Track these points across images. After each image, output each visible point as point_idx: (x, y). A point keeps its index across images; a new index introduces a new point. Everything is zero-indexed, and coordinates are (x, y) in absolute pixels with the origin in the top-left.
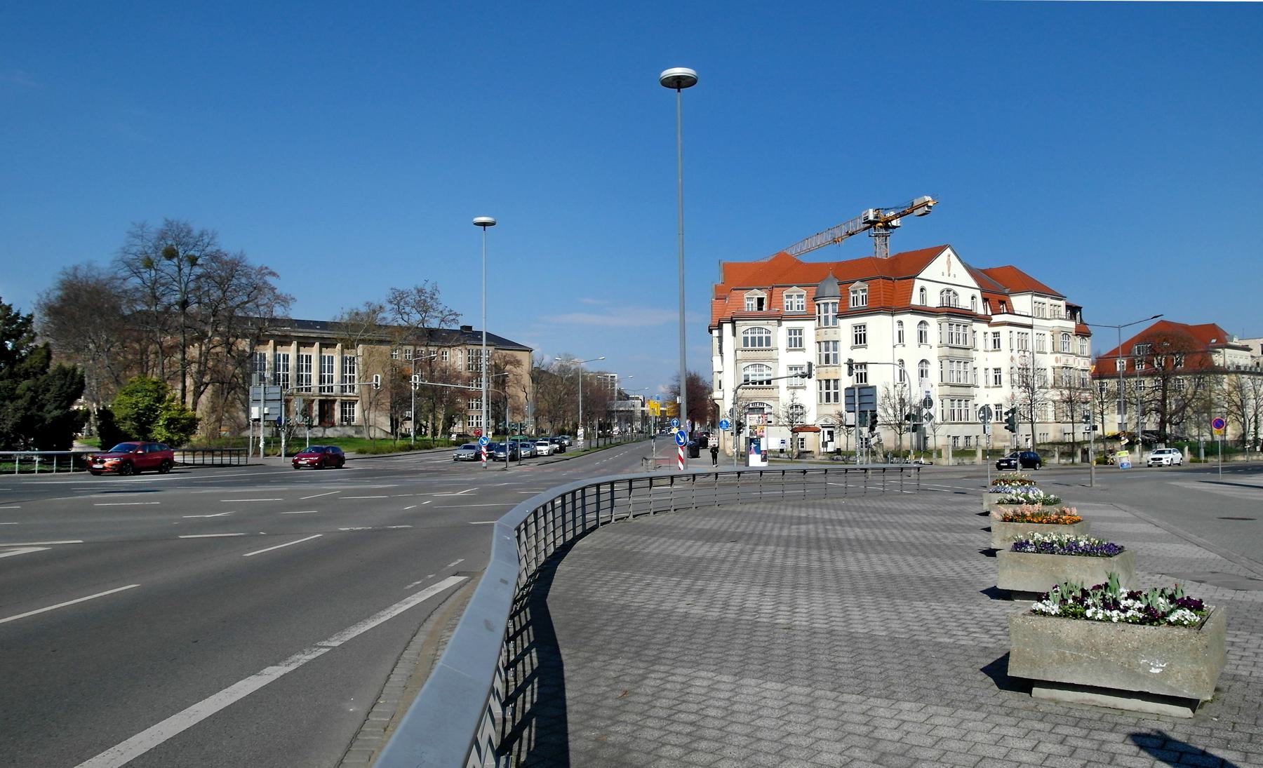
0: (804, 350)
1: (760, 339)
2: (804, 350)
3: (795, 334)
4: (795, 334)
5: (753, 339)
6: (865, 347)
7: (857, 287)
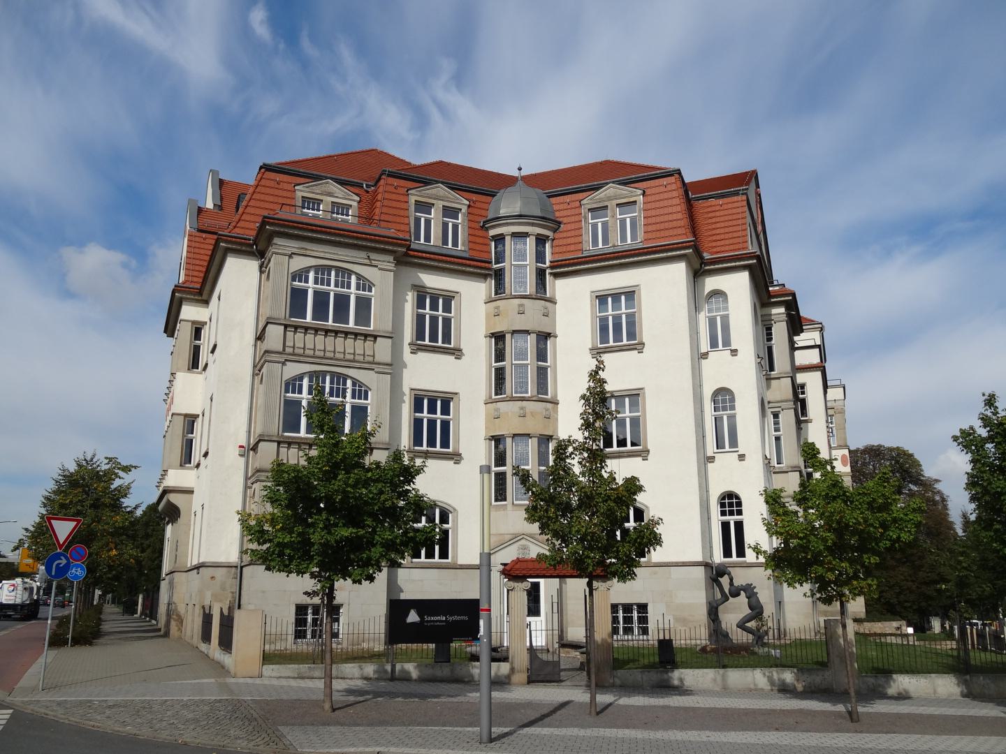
0: (457, 353)
1: (342, 301)
2: (457, 353)
3: (434, 307)
4: (434, 307)
5: (321, 299)
6: (639, 347)
7: (609, 199)
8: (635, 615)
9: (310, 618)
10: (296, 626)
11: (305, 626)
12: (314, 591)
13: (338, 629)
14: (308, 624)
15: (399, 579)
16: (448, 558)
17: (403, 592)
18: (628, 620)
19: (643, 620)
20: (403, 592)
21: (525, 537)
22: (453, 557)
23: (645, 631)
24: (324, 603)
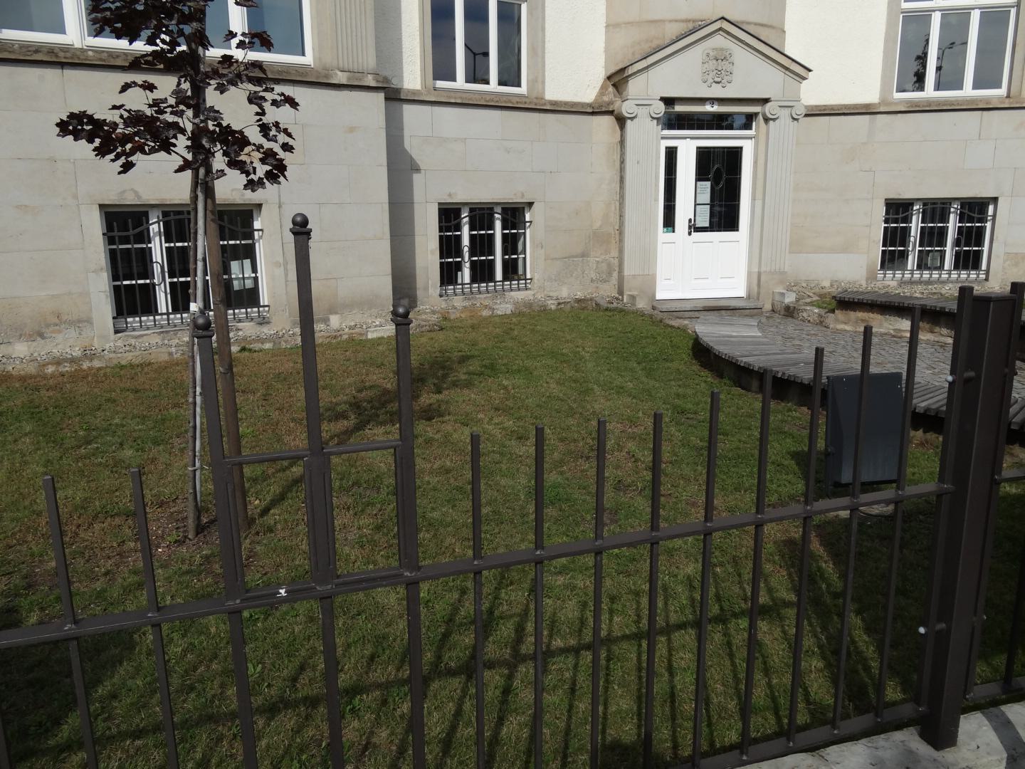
8: (953, 225)
9: (158, 249)
10: (115, 277)
11: (147, 273)
12: (135, 119)
13: (256, 279)
14: (157, 269)
15: (407, 133)
16: (519, 85)
17: (418, 170)
18: (933, 237)
19: (972, 237)
20: (418, 170)
21: (726, 26)
22: (532, 83)
23: (968, 260)
24: (209, 192)
